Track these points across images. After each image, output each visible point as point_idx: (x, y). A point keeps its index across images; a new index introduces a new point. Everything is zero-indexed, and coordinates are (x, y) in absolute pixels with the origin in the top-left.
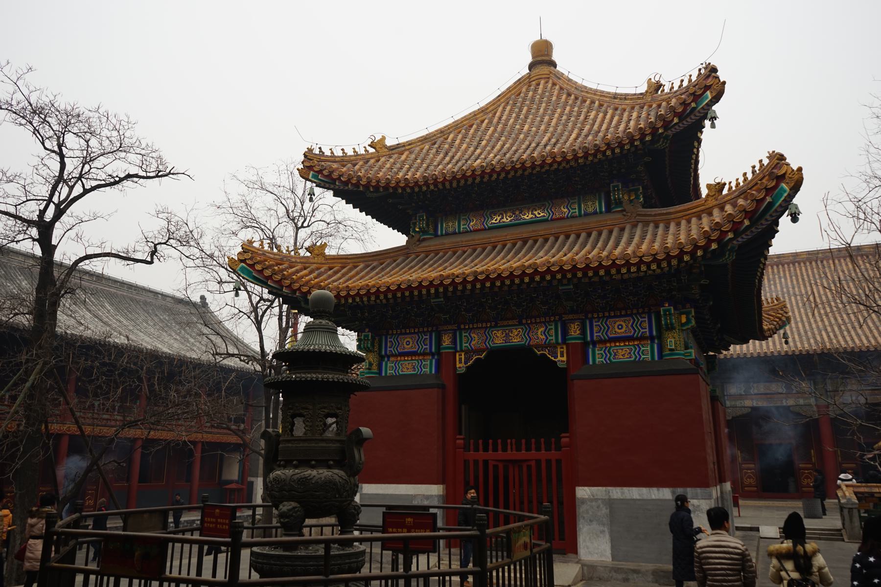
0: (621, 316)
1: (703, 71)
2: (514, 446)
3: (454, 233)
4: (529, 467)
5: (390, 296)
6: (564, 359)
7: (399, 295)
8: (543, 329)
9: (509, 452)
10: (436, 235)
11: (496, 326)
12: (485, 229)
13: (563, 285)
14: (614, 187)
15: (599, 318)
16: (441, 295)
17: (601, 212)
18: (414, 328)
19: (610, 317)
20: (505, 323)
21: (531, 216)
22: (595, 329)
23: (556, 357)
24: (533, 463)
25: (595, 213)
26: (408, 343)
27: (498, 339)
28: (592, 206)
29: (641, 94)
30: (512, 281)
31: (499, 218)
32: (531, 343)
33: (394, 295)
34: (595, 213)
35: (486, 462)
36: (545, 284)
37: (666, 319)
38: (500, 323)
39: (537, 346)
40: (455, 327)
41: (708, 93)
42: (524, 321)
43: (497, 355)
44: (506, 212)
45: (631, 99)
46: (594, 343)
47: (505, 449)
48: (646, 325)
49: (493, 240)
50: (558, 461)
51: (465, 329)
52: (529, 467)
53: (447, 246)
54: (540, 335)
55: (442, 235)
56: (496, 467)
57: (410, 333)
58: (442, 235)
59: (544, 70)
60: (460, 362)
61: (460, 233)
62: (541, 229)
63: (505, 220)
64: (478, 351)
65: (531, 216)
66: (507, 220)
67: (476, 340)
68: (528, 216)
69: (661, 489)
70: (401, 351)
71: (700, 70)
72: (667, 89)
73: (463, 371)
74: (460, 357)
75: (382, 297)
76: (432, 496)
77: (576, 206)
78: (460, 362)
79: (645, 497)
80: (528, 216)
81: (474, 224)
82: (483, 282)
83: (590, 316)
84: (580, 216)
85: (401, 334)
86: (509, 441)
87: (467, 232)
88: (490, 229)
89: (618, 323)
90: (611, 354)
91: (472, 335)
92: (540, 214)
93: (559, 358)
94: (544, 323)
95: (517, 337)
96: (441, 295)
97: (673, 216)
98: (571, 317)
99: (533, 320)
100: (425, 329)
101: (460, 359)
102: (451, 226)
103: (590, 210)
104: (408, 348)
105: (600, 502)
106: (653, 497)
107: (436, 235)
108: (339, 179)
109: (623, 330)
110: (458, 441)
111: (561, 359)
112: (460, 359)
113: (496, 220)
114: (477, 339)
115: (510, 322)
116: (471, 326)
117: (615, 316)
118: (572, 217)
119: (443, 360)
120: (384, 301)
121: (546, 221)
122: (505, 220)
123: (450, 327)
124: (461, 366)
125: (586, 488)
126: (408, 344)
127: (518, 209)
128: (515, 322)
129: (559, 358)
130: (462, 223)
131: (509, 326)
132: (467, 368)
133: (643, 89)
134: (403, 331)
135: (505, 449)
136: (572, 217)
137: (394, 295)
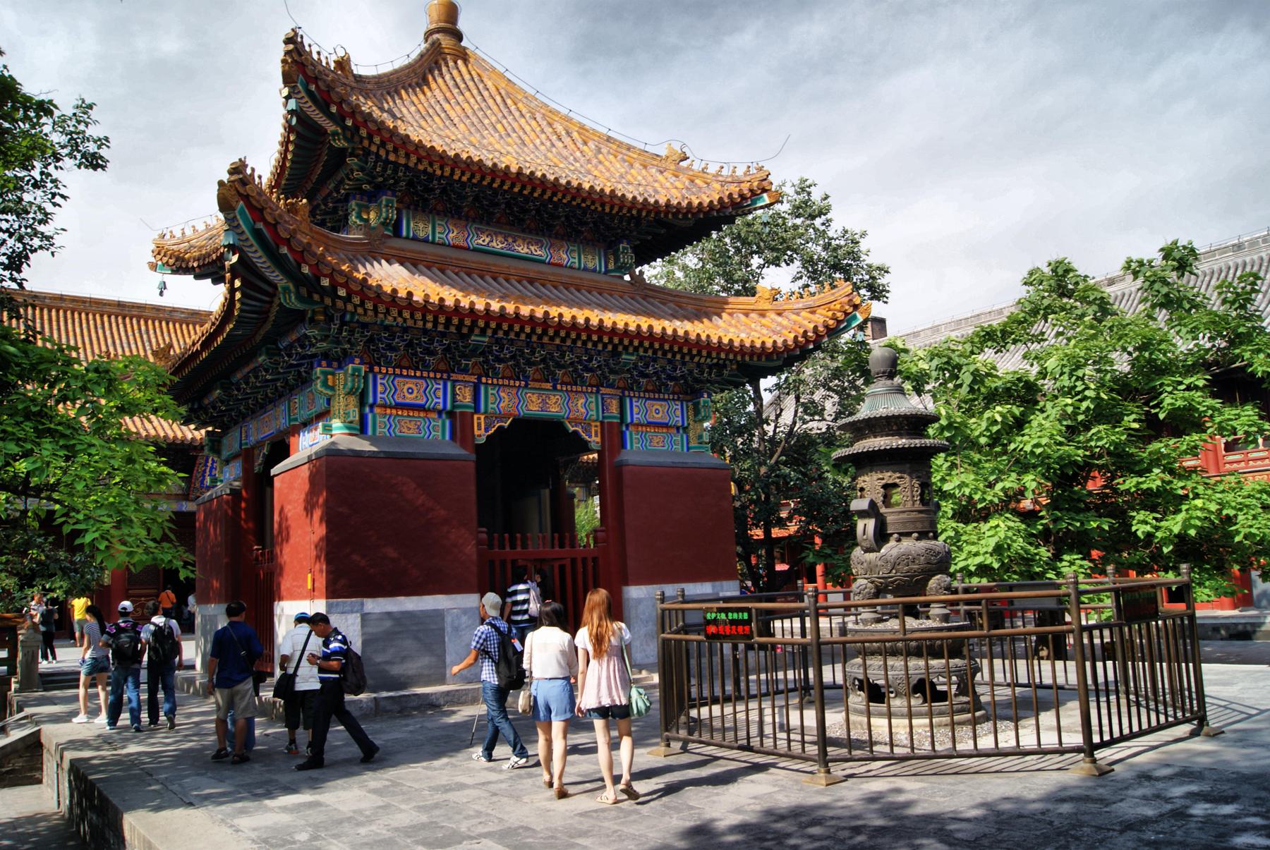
0: (659, 399)
3: (425, 241)
4: (562, 568)
6: (598, 439)
8: (583, 401)
13: (628, 354)
15: (639, 397)
16: (489, 332)
18: (417, 369)
19: (649, 399)
20: (537, 385)
21: (526, 250)
24: (568, 562)
26: (410, 391)
31: (487, 240)
34: (594, 271)
38: (532, 384)
39: (576, 422)
40: (474, 379)
41: (765, 195)
42: (559, 387)
44: (496, 234)
48: (679, 413)
49: (493, 269)
52: (562, 568)
53: (430, 258)
55: (407, 238)
60: (479, 429)
63: (494, 244)
64: (502, 417)
65: (526, 250)
66: (498, 245)
68: (522, 250)
70: (400, 400)
73: (482, 440)
74: (479, 420)
77: (576, 255)
78: (479, 429)
80: (522, 250)
81: (454, 236)
85: (401, 375)
87: (443, 245)
88: (475, 250)
91: (502, 394)
93: (593, 438)
98: (608, 391)
100: (425, 374)
101: (479, 425)
103: (590, 265)
104: (410, 399)
112: (479, 425)
115: (545, 385)
118: (571, 268)
119: (459, 422)
121: (543, 262)
122: (494, 244)
123: (467, 378)
124: (481, 434)
127: (510, 235)
128: (549, 386)
130: (438, 230)
134: (398, 371)
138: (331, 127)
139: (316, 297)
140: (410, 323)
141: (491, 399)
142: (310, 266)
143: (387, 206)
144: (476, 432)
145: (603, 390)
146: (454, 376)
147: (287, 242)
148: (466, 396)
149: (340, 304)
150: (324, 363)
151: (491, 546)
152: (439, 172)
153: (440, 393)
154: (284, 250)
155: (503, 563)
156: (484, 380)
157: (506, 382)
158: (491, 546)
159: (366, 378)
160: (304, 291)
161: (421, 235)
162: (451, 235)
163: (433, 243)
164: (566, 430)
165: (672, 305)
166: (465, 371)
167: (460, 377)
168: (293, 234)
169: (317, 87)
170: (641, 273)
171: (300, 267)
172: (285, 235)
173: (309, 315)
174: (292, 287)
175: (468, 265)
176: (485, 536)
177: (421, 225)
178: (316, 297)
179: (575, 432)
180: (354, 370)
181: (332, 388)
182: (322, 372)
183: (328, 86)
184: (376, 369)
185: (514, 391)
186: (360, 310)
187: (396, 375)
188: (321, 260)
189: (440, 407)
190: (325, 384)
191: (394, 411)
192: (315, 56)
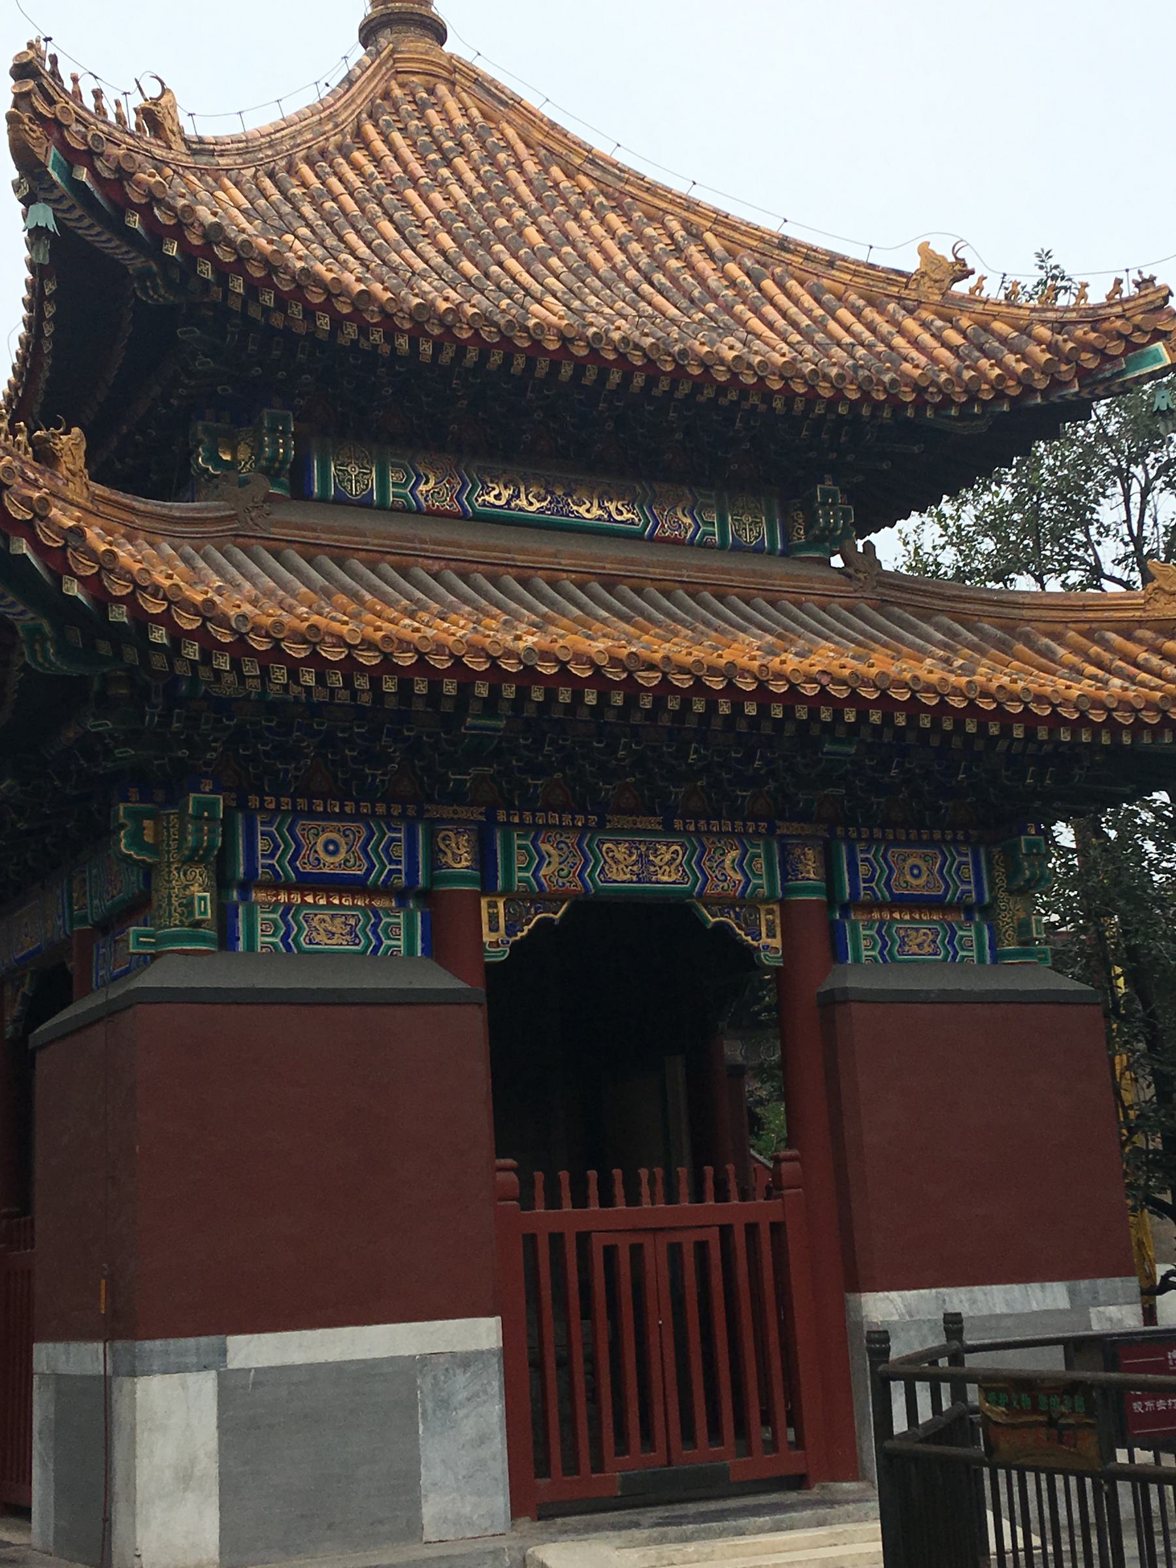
0: (920, 843)
1: (1129, 290)
2: (660, 1188)
3: (364, 503)
4: (701, 1247)
5: (389, 685)
6: (777, 942)
7: (421, 688)
9: (646, 1205)
10: (300, 491)
11: (601, 825)
12: (463, 517)
13: (839, 741)
14: (826, 494)
15: (871, 840)
16: (505, 709)
17: (772, 551)
19: (897, 843)
20: (626, 822)
21: (596, 512)
22: (863, 869)
23: (757, 936)
25: (758, 550)
26: (332, 848)
27: (619, 867)
28: (753, 529)
29: (900, 273)
30: (764, 710)
31: (506, 494)
32: (708, 890)
33: (405, 685)
34: (758, 550)
35: (583, 1239)
36: (767, 729)
37: (1031, 866)
38: (615, 821)
39: (723, 903)
42: (678, 824)
43: (597, 913)
45: (855, 273)
46: (854, 904)
47: (633, 1199)
48: (969, 873)
50: (777, 1228)
51: (522, 824)
53: (373, 543)
54: (728, 869)
56: (610, 1252)
57: (342, 816)
58: (323, 499)
59: (415, 45)
61: (382, 507)
62: (610, 558)
64: (543, 898)
65: (596, 512)
66: (530, 504)
67: (551, 864)
68: (589, 511)
69: (1047, 1284)
71: (1118, 282)
72: (993, 291)
73: (501, 955)
75: (362, 683)
76: (478, 1355)
78: (494, 928)
79: (1019, 1308)
80: (589, 511)
82: (686, 697)
83: (840, 831)
84: (723, 546)
85: (311, 814)
86: (644, 1173)
87: (406, 510)
89: (910, 861)
90: (893, 941)
91: (545, 847)
92: (624, 514)
93: (765, 940)
94: (740, 836)
95: (668, 869)
96: (505, 709)
97: (1027, 613)
98: (794, 828)
99: (528, 819)
101: (493, 918)
102: (358, 478)
103: (748, 537)
104: (330, 864)
105: (925, 1329)
106: (1035, 1307)
107: (300, 491)
108: (145, 210)
109: (922, 881)
110: (500, 1176)
111: (769, 944)
112: (493, 918)
113: (496, 496)
114: (556, 859)
115: (644, 822)
116: (528, 819)
117: (909, 844)
118: (703, 545)
120: (343, 696)
121: (635, 537)
123: (464, 813)
125: (893, 1294)
126: (331, 849)
128: (653, 823)
129: (765, 940)
130: (392, 477)
131: (644, 832)
132: (515, 946)
133: (911, 264)
134: (302, 803)
135: (633, 1199)
136: (703, 545)
137: (405, 685)
138: (135, 262)
139: (104, 648)
140: (320, 696)
141: (519, 860)
142: (82, 580)
143: (273, 430)
144: (488, 937)
145: (783, 828)
146: (434, 811)
147: (27, 529)
148: (460, 857)
149: (159, 662)
150: (134, 793)
151: (527, 1202)
152: (386, 349)
153: (400, 852)
154: (23, 547)
155: (556, 1240)
156: (502, 816)
157: (554, 819)
158: (527, 1202)
159: (228, 823)
160: (75, 636)
161: (354, 490)
162: (422, 487)
163: (382, 507)
164: (700, 922)
165: (945, 620)
166: (458, 797)
167: (447, 812)
168: (40, 510)
169: (94, 173)
170: (870, 547)
171: (59, 582)
172: (20, 514)
173: (96, 686)
174: (47, 628)
175: (459, 553)
176: (512, 1176)
177: (354, 471)
178: (104, 648)
179: (721, 927)
180: (200, 805)
181: (154, 849)
182: (130, 814)
183: (119, 169)
184: (254, 801)
185: (572, 840)
186: (204, 673)
187: (297, 814)
188: (107, 563)
189: (401, 881)
190: (136, 840)
191: (296, 898)
192: (89, 102)
